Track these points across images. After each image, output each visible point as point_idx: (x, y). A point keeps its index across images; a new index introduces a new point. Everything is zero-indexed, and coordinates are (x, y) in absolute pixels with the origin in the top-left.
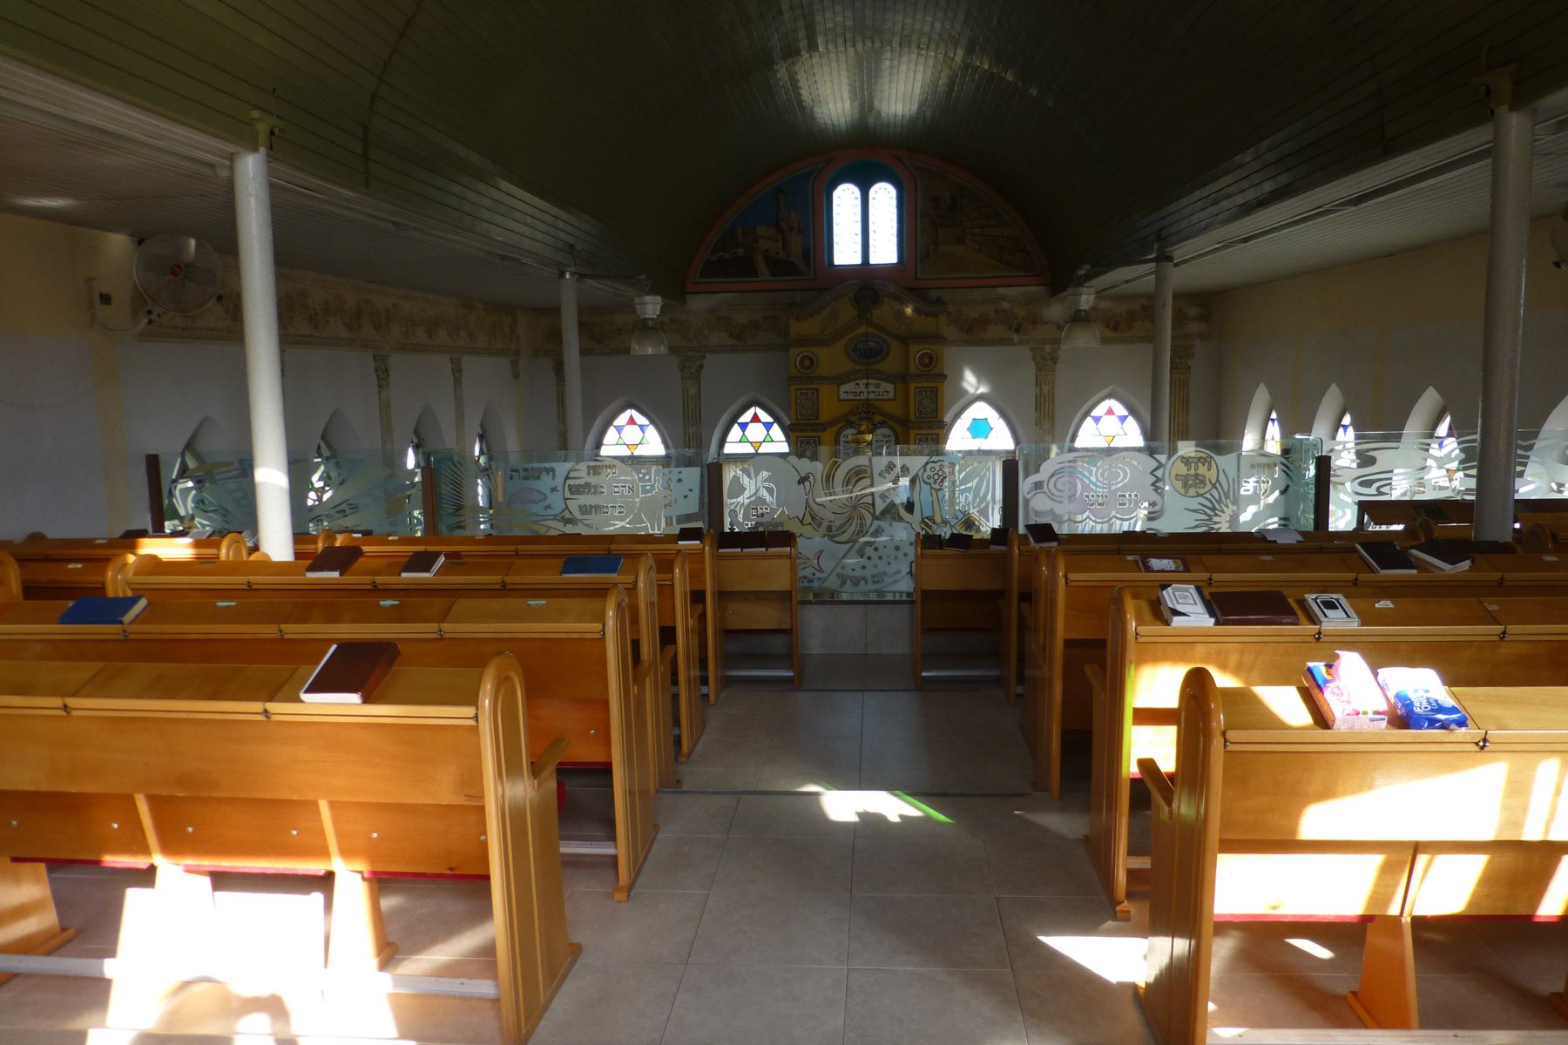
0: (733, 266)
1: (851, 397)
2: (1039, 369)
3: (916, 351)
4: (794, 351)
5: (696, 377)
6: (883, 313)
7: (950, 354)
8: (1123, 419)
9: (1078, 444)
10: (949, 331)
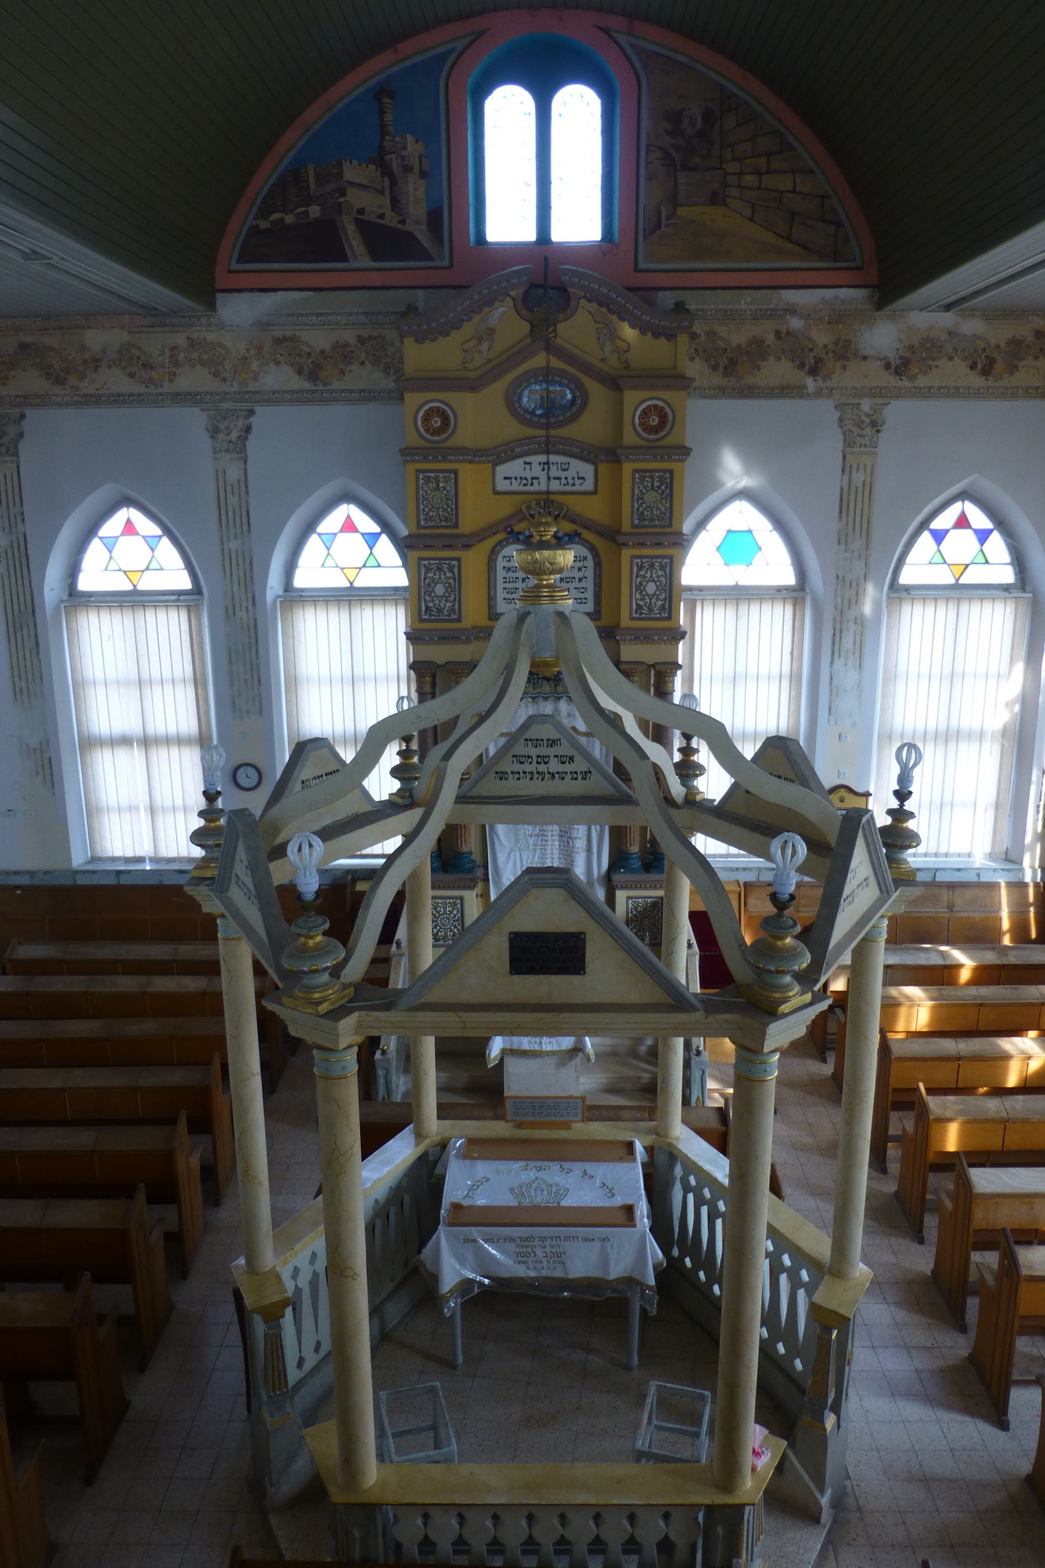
0: (305, 243)
1: (516, 486)
2: (848, 443)
3: (636, 401)
4: (413, 399)
5: (239, 448)
6: (578, 329)
7: (698, 415)
8: (983, 536)
9: (904, 579)
10: (694, 369)
